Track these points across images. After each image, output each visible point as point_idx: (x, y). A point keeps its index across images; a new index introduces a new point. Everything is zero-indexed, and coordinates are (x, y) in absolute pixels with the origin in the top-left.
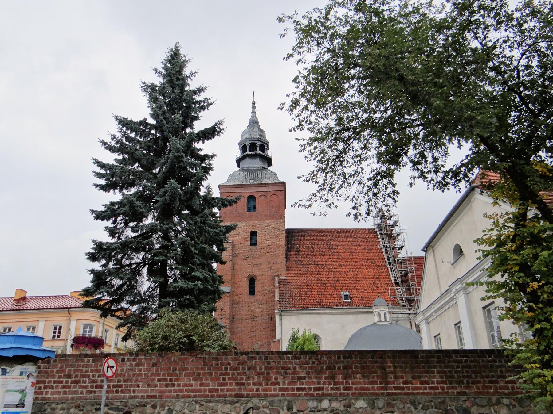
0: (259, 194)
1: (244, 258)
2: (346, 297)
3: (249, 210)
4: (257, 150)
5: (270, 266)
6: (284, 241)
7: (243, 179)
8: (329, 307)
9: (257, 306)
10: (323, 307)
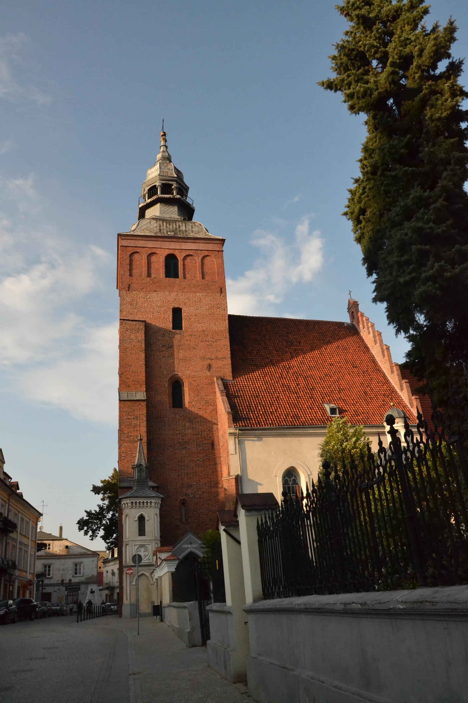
0: (184, 254)
1: (164, 349)
3: (168, 275)
6: (227, 324)
7: (156, 230)
8: (312, 426)
9: (188, 425)
10: (304, 426)
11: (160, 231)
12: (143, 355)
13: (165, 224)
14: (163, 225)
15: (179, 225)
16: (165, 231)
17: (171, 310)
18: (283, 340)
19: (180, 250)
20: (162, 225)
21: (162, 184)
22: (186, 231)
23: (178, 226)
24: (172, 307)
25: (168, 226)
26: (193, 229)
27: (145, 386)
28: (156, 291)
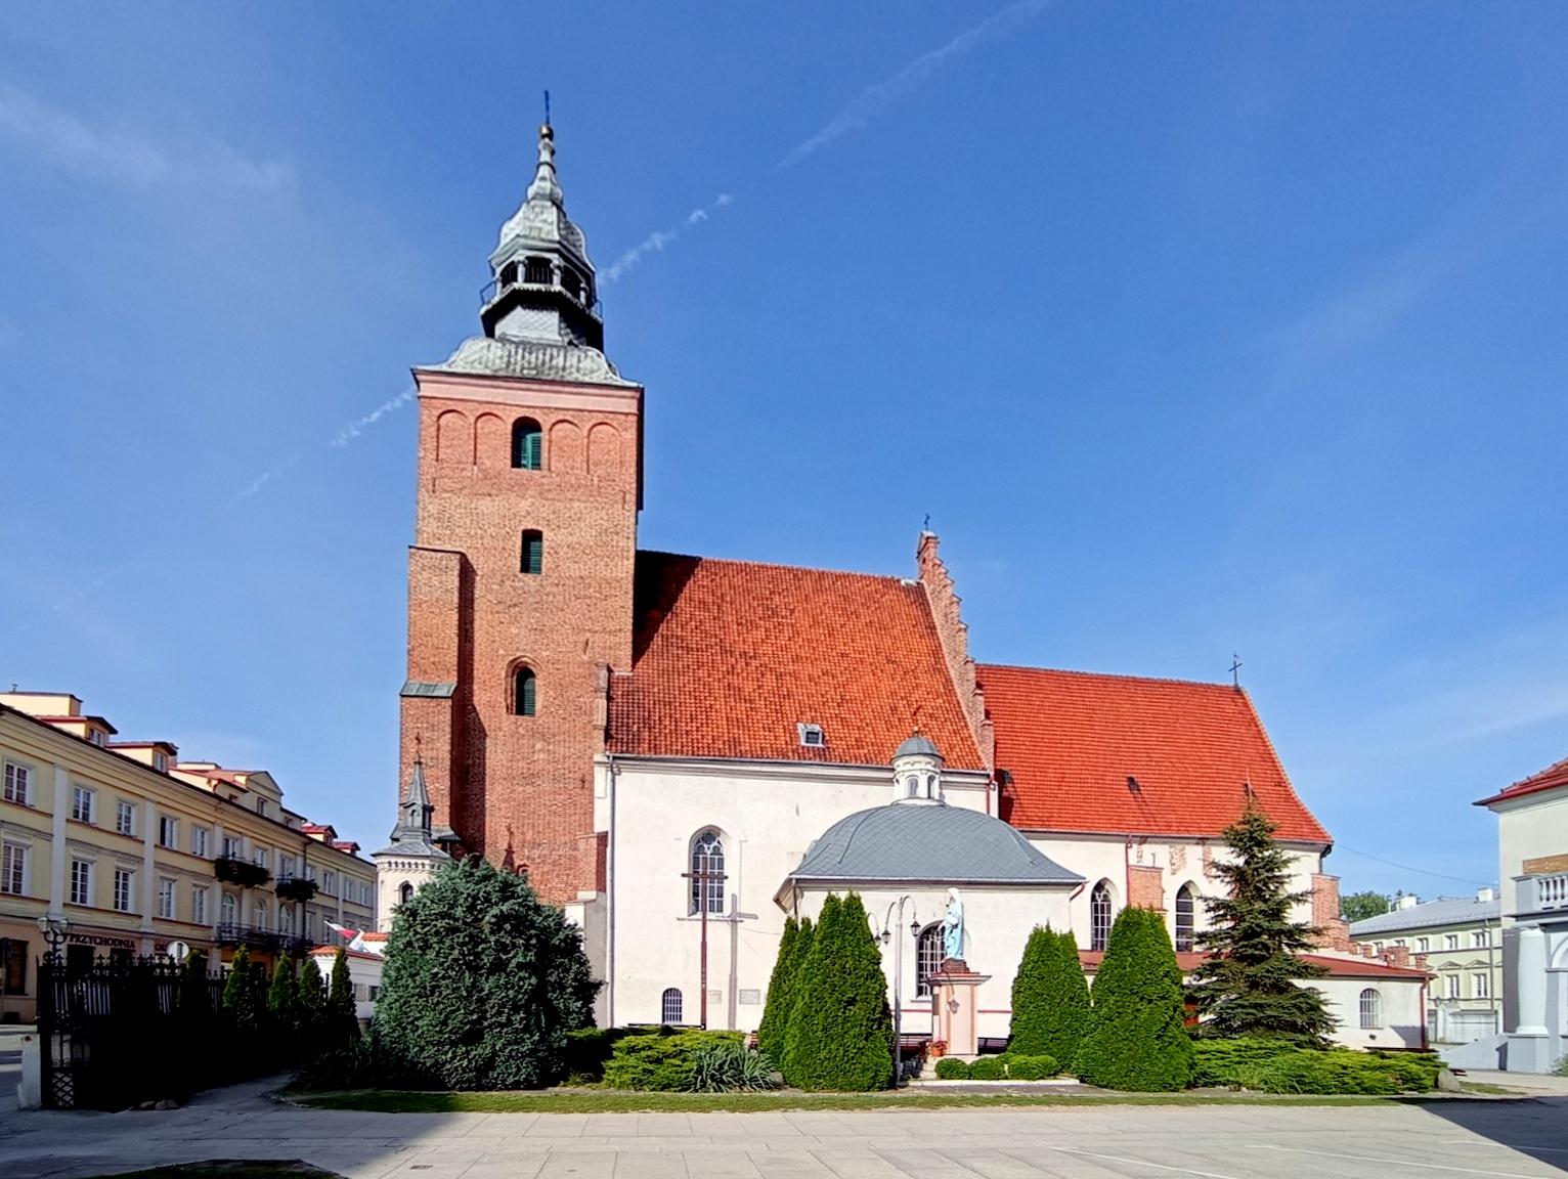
1: (500, 608)
2: (811, 736)
4: (551, 282)
5: (583, 639)
6: (632, 567)
8: (758, 757)
11: (508, 366)
12: (456, 617)
13: (520, 351)
14: (516, 352)
15: (552, 356)
16: (518, 368)
17: (520, 534)
18: (759, 605)
19: (546, 411)
20: (513, 353)
21: (528, 258)
22: (564, 369)
23: (548, 357)
24: (523, 528)
25: (527, 355)
26: (581, 365)
27: (455, 673)
28: (490, 495)
